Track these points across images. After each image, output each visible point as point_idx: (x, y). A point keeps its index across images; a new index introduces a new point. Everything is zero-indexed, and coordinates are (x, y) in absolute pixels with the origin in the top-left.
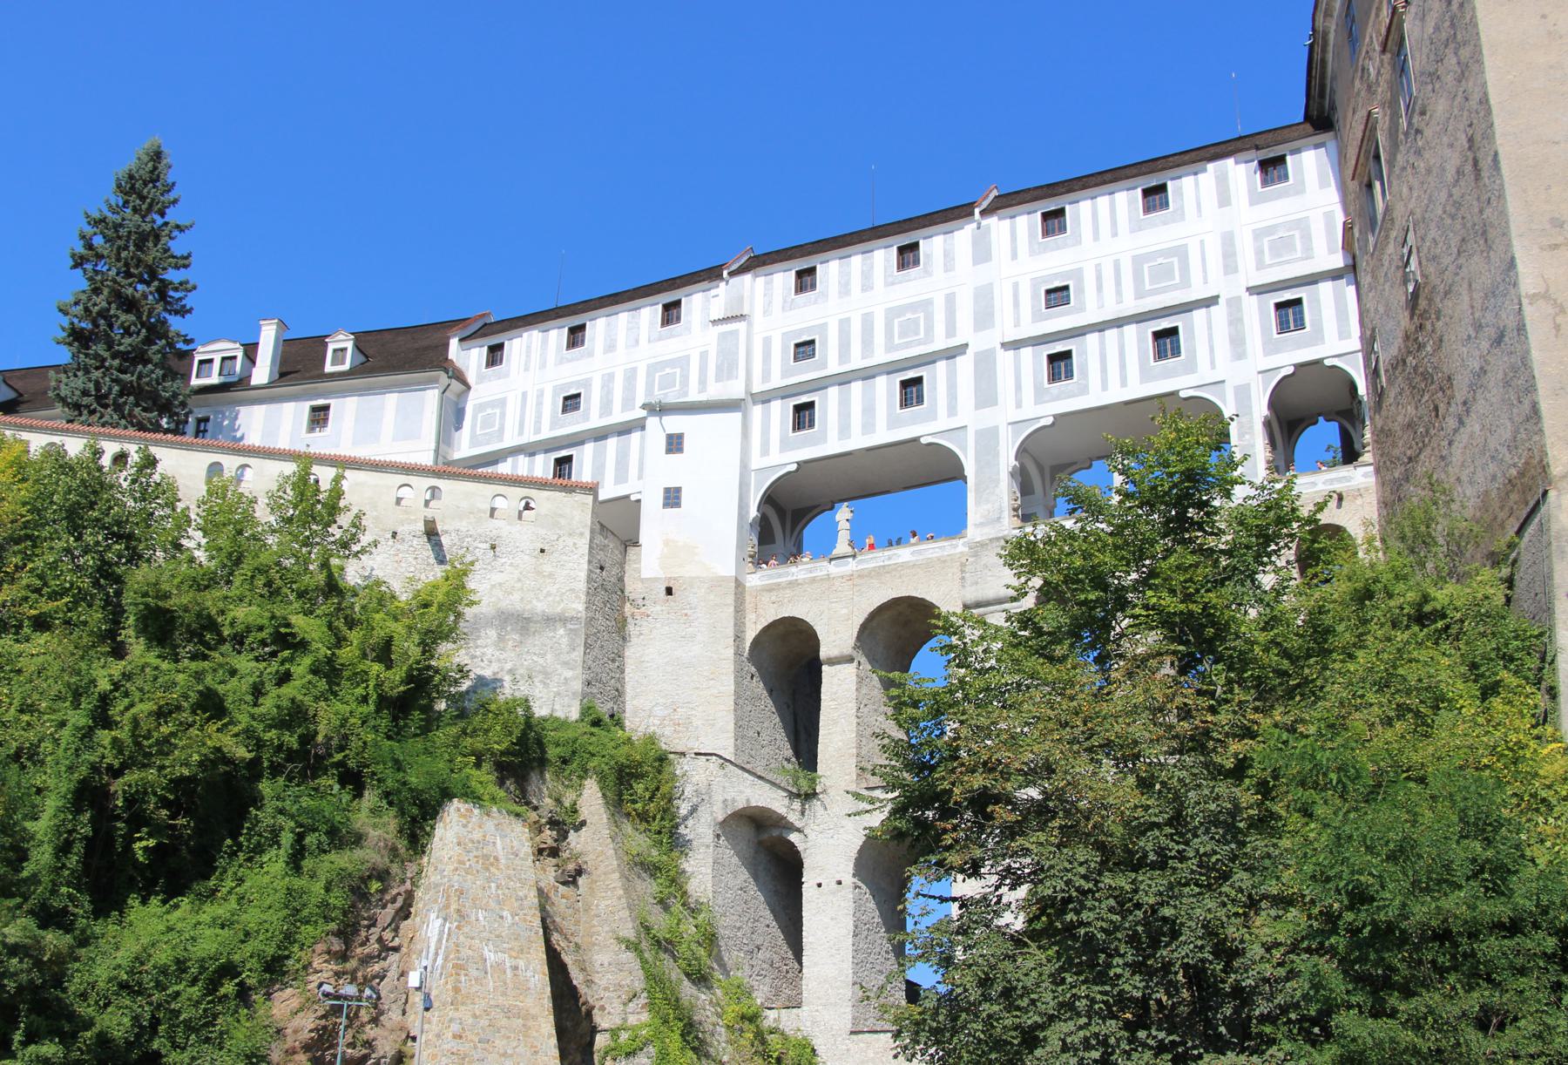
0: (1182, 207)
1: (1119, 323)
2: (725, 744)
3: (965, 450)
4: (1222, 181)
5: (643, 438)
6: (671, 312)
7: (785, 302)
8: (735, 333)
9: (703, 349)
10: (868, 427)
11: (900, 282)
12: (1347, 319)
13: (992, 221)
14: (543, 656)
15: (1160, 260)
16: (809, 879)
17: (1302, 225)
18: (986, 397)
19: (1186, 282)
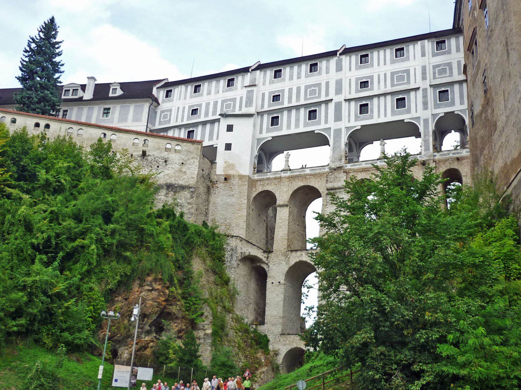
0: (409, 56)
1: (385, 95)
2: (241, 232)
3: (330, 136)
4: (423, 48)
5: (219, 125)
6: (230, 83)
7: (270, 81)
8: (253, 91)
9: (241, 96)
10: (297, 126)
11: (311, 77)
12: (463, 98)
13: (343, 57)
14: (181, 199)
15: (400, 74)
16: (269, 281)
17: (450, 65)
18: (338, 118)
19: (409, 82)
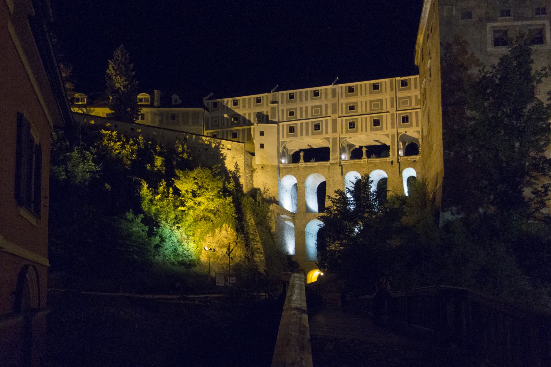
7: (286, 101)
15: (376, 102)
17: (410, 98)
19: (382, 108)
